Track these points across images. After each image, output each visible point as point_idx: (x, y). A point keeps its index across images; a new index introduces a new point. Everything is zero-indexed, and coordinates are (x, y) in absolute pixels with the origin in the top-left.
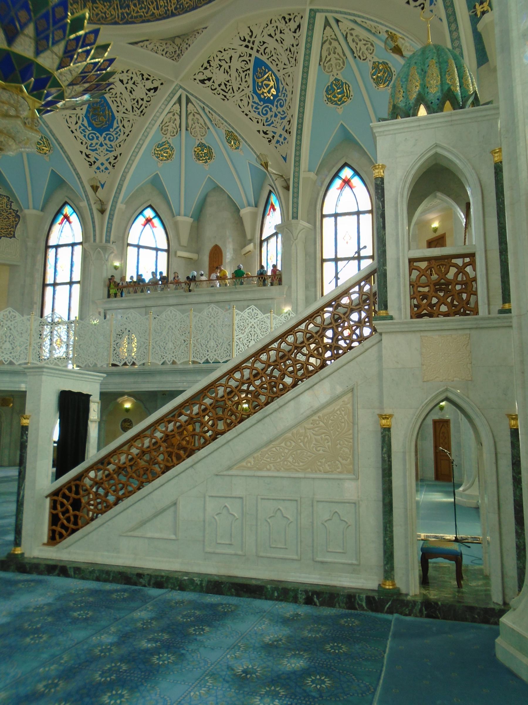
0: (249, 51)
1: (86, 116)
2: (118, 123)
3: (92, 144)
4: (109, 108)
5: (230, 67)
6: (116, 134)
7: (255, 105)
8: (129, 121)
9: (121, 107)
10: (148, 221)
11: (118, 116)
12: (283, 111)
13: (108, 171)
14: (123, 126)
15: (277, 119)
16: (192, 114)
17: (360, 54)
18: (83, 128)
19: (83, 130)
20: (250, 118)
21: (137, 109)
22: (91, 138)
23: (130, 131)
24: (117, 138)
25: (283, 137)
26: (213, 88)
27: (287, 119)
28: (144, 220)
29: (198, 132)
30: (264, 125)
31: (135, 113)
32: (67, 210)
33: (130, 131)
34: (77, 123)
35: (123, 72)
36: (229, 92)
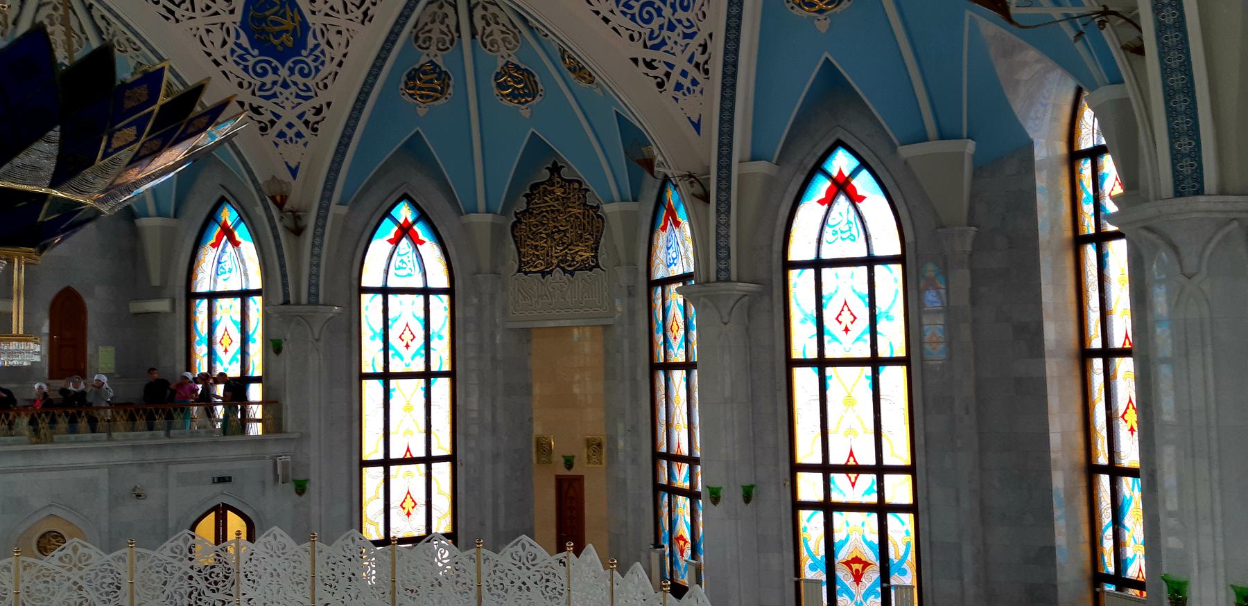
1: (244, 25)
2: (315, 37)
3: (264, 84)
6: (314, 61)
8: (339, 32)
10: (405, 231)
11: (315, 22)
12: (688, 20)
13: (303, 140)
14: (329, 43)
15: (673, 35)
16: (480, 7)
18: (240, 52)
19: (240, 57)
20: (614, 29)
21: (354, 8)
22: (259, 71)
23: (345, 55)
27: (699, 39)
28: (396, 228)
29: (500, 42)
30: (645, 46)
31: (350, 16)
32: (229, 215)
33: (345, 55)
34: (224, 43)
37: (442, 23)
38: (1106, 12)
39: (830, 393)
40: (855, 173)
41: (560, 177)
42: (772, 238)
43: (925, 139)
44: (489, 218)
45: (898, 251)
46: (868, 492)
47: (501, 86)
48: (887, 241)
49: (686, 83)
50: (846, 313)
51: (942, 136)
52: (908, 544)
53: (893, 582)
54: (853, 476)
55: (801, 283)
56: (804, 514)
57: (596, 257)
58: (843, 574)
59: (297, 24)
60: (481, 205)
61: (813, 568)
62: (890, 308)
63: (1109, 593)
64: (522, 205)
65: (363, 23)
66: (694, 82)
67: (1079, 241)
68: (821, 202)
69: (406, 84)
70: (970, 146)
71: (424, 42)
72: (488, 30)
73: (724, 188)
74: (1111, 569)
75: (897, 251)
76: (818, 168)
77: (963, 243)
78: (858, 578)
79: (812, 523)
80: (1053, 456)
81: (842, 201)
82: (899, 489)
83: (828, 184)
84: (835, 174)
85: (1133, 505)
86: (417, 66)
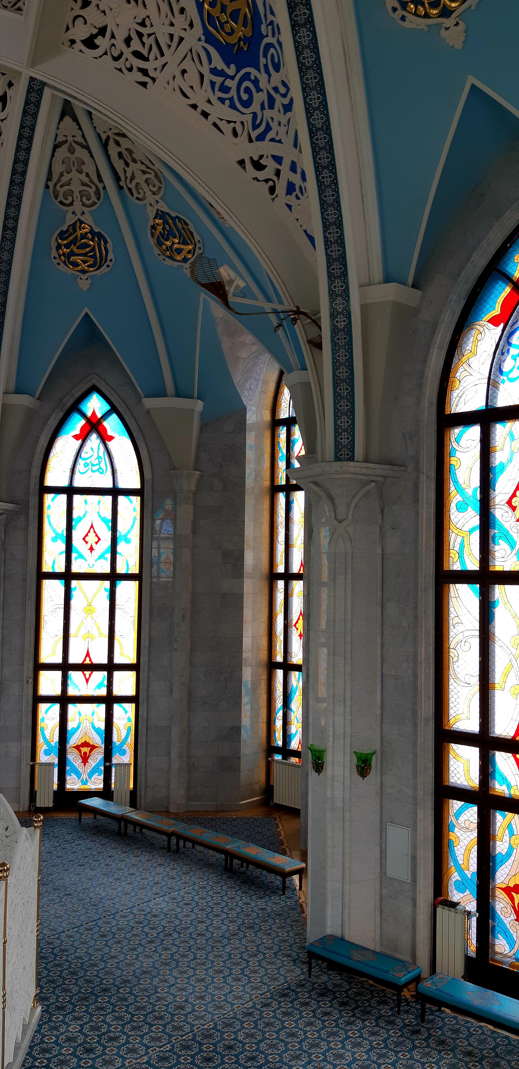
17: (132, 186)
38: (298, 312)
39: (73, 603)
40: (106, 416)
42: (30, 464)
43: (165, 395)
45: (137, 485)
46: (99, 686)
48: (130, 478)
50: (92, 534)
51: (178, 394)
52: (129, 729)
53: (114, 761)
54: (87, 673)
55: (55, 506)
56: (43, 707)
58: (73, 757)
61: (47, 753)
62: (129, 532)
63: (277, 761)
67: (275, 489)
68: (76, 437)
70: (199, 405)
74: (280, 743)
75: (137, 485)
76: (75, 408)
77: (189, 484)
78: (85, 759)
79: (49, 715)
80: (245, 655)
81: (94, 439)
82: (125, 683)
83: (83, 422)
84: (89, 414)
85: (297, 694)
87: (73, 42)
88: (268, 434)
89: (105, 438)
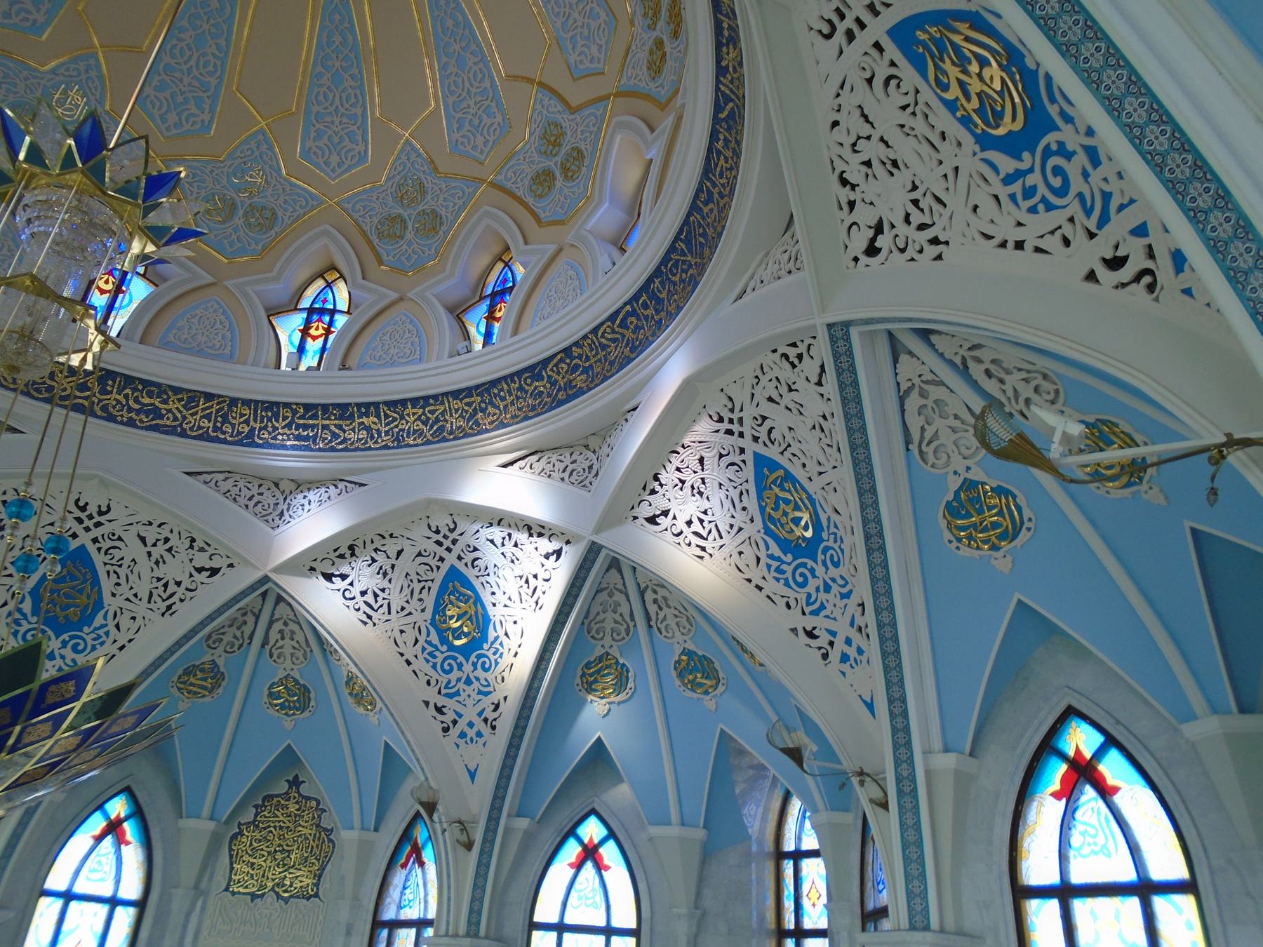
0: (441, 551)
2: (105, 617)
4: (96, 582)
5: (393, 567)
6: (94, 639)
7: (430, 649)
8: (134, 618)
9: (124, 588)
14: (117, 626)
23: (130, 641)
24: (94, 648)
25: (475, 729)
26: (347, 595)
30: (439, 693)
31: (151, 606)
33: (130, 641)
35: (150, 524)
36: (381, 611)
37: (239, 628)
41: (298, 792)
44: (212, 825)
45: (633, 925)
47: (271, 695)
49: (471, 733)
57: (317, 885)
59: (92, 601)
60: (206, 811)
64: (249, 815)
65: (163, 615)
66: (479, 734)
69: (180, 677)
71: (214, 642)
72: (280, 643)
73: (488, 840)
75: (633, 925)
76: (572, 832)
86: (197, 663)
87: (635, 518)
88: (770, 865)
89: (600, 867)
